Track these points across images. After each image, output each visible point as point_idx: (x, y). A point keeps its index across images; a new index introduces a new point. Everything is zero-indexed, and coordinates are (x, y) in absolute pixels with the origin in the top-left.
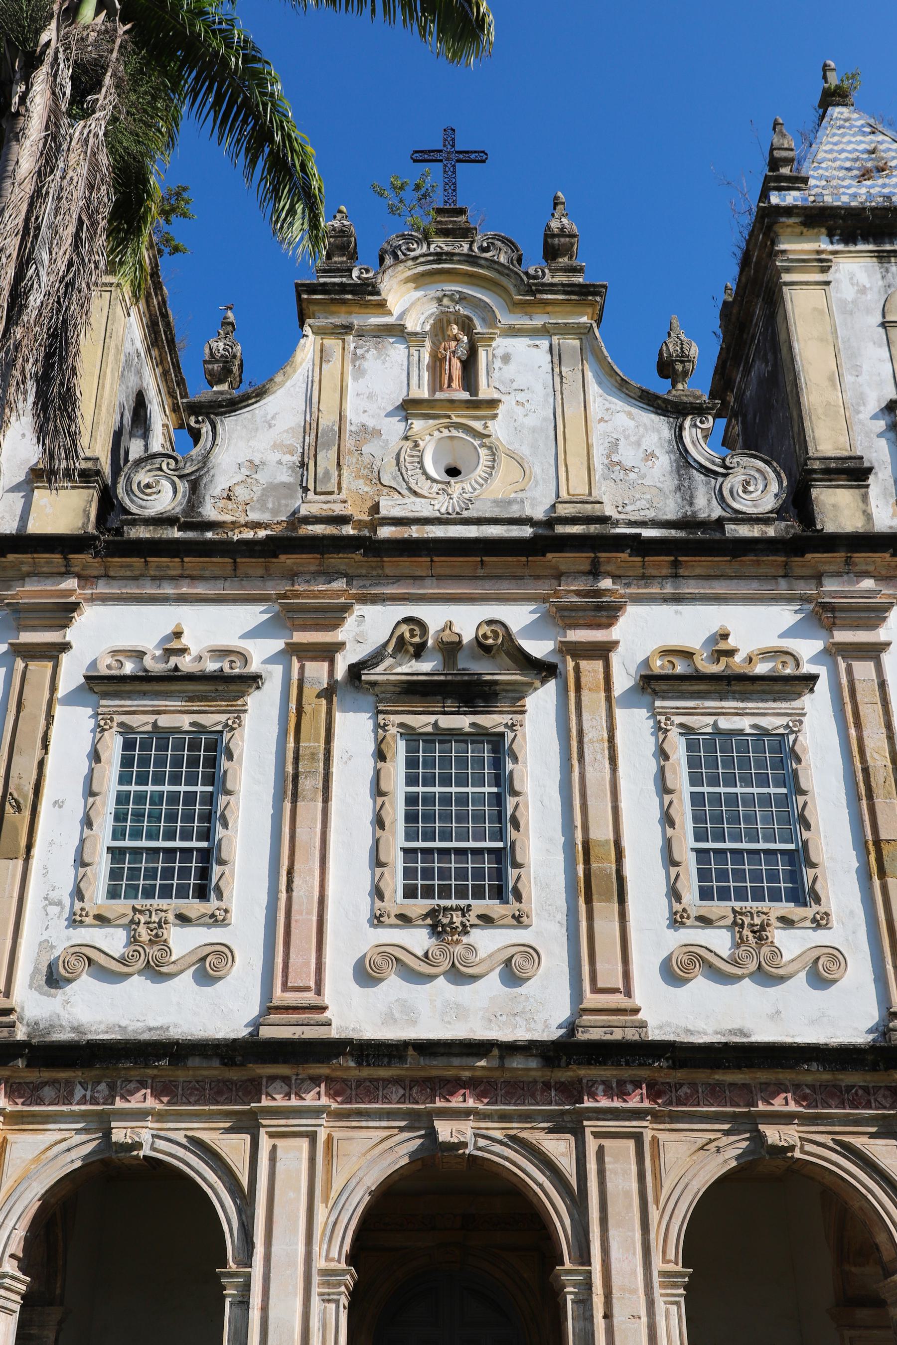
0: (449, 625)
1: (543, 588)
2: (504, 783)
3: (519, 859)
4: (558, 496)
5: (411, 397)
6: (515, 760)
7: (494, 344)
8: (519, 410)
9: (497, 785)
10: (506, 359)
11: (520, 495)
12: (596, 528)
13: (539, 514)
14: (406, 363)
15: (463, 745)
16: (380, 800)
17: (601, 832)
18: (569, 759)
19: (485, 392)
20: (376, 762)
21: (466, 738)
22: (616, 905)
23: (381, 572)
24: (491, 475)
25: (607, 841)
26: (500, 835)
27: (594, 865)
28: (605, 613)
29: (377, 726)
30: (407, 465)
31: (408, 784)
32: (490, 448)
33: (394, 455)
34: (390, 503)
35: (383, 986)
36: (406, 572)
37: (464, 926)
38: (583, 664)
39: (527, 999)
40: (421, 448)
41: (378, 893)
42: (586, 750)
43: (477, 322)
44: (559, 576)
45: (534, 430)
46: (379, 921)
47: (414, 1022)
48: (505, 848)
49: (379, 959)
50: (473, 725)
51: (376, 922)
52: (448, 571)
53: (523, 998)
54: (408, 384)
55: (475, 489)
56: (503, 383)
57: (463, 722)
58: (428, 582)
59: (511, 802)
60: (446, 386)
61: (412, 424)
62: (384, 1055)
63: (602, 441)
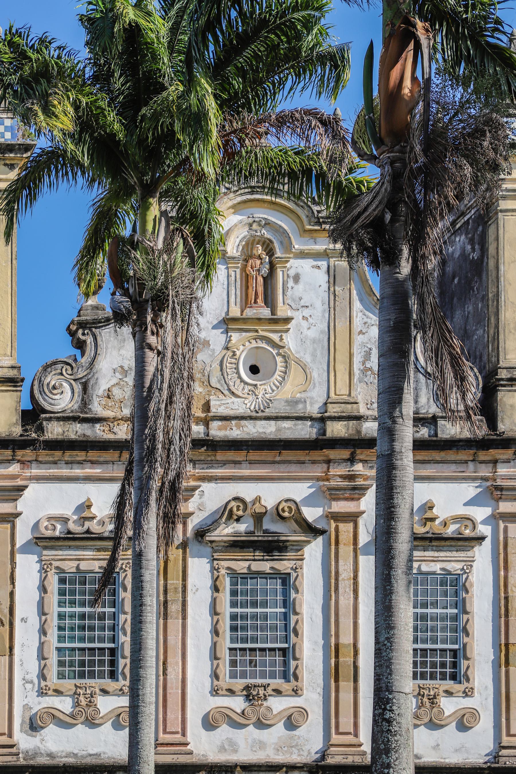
0: (258, 499)
1: (318, 471)
2: (289, 606)
3: (297, 656)
4: (328, 397)
5: (231, 315)
6: (297, 591)
7: (288, 265)
8: (305, 324)
9: (285, 607)
10: (297, 278)
11: (303, 395)
12: (353, 424)
13: (314, 410)
14: (226, 283)
15: (265, 580)
16: (216, 618)
17: (346, 639)
18: (330, 591)
19: (282, 311)
20: (213, 593)
21: (266, 576)
22: (352, 683)
23: (213, 458)
24: (284, 379)
25: (349, 644)
26: (286, 639)
27: (341, 659)
28: (357, 491)
29: (214, 569)
30: (228, 370)
31: (231, 607)
32: (284, 357)
33: (218, 362)
34: (218, 403)
35: (219, 730)
36: (230, 458)
37: (265, 696)
38: (341, 526)
39: (299, 738)
40: (237, 357)
41: (215, 676)
42: (340, 585)
43: (276, 245)
44: (328, 462)
45: (314, 341)
46: (217, 693)
47: (236, 751)
48: (288, 648)
49: (217, 716)
50: (272, 568)
51: (214, 693)
52: (257, 458)
53: (296, 737)
54: (228, 301)
55: (273, 391)
56: (294, 300)
57: (266, 566)
58: (244, 465)
59: (293, 618)
60: (253, 301)
61: (231, 336)
62: (223, 771)
63: (359, 351)
